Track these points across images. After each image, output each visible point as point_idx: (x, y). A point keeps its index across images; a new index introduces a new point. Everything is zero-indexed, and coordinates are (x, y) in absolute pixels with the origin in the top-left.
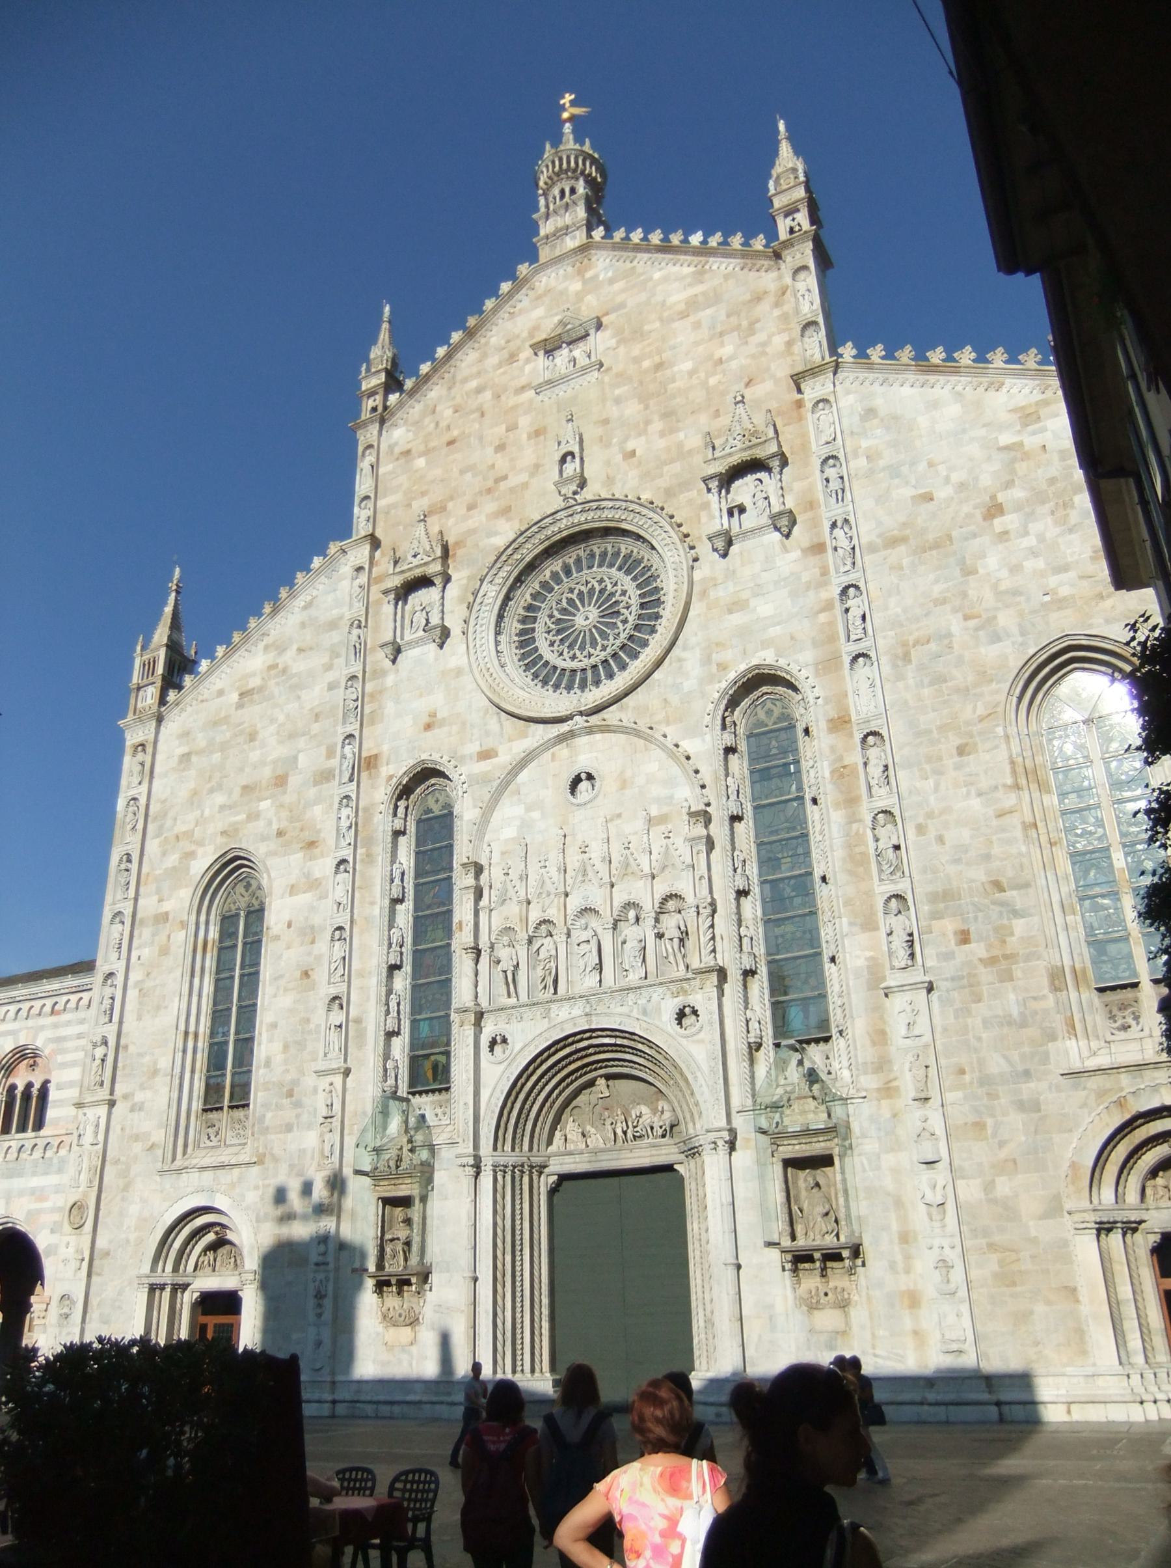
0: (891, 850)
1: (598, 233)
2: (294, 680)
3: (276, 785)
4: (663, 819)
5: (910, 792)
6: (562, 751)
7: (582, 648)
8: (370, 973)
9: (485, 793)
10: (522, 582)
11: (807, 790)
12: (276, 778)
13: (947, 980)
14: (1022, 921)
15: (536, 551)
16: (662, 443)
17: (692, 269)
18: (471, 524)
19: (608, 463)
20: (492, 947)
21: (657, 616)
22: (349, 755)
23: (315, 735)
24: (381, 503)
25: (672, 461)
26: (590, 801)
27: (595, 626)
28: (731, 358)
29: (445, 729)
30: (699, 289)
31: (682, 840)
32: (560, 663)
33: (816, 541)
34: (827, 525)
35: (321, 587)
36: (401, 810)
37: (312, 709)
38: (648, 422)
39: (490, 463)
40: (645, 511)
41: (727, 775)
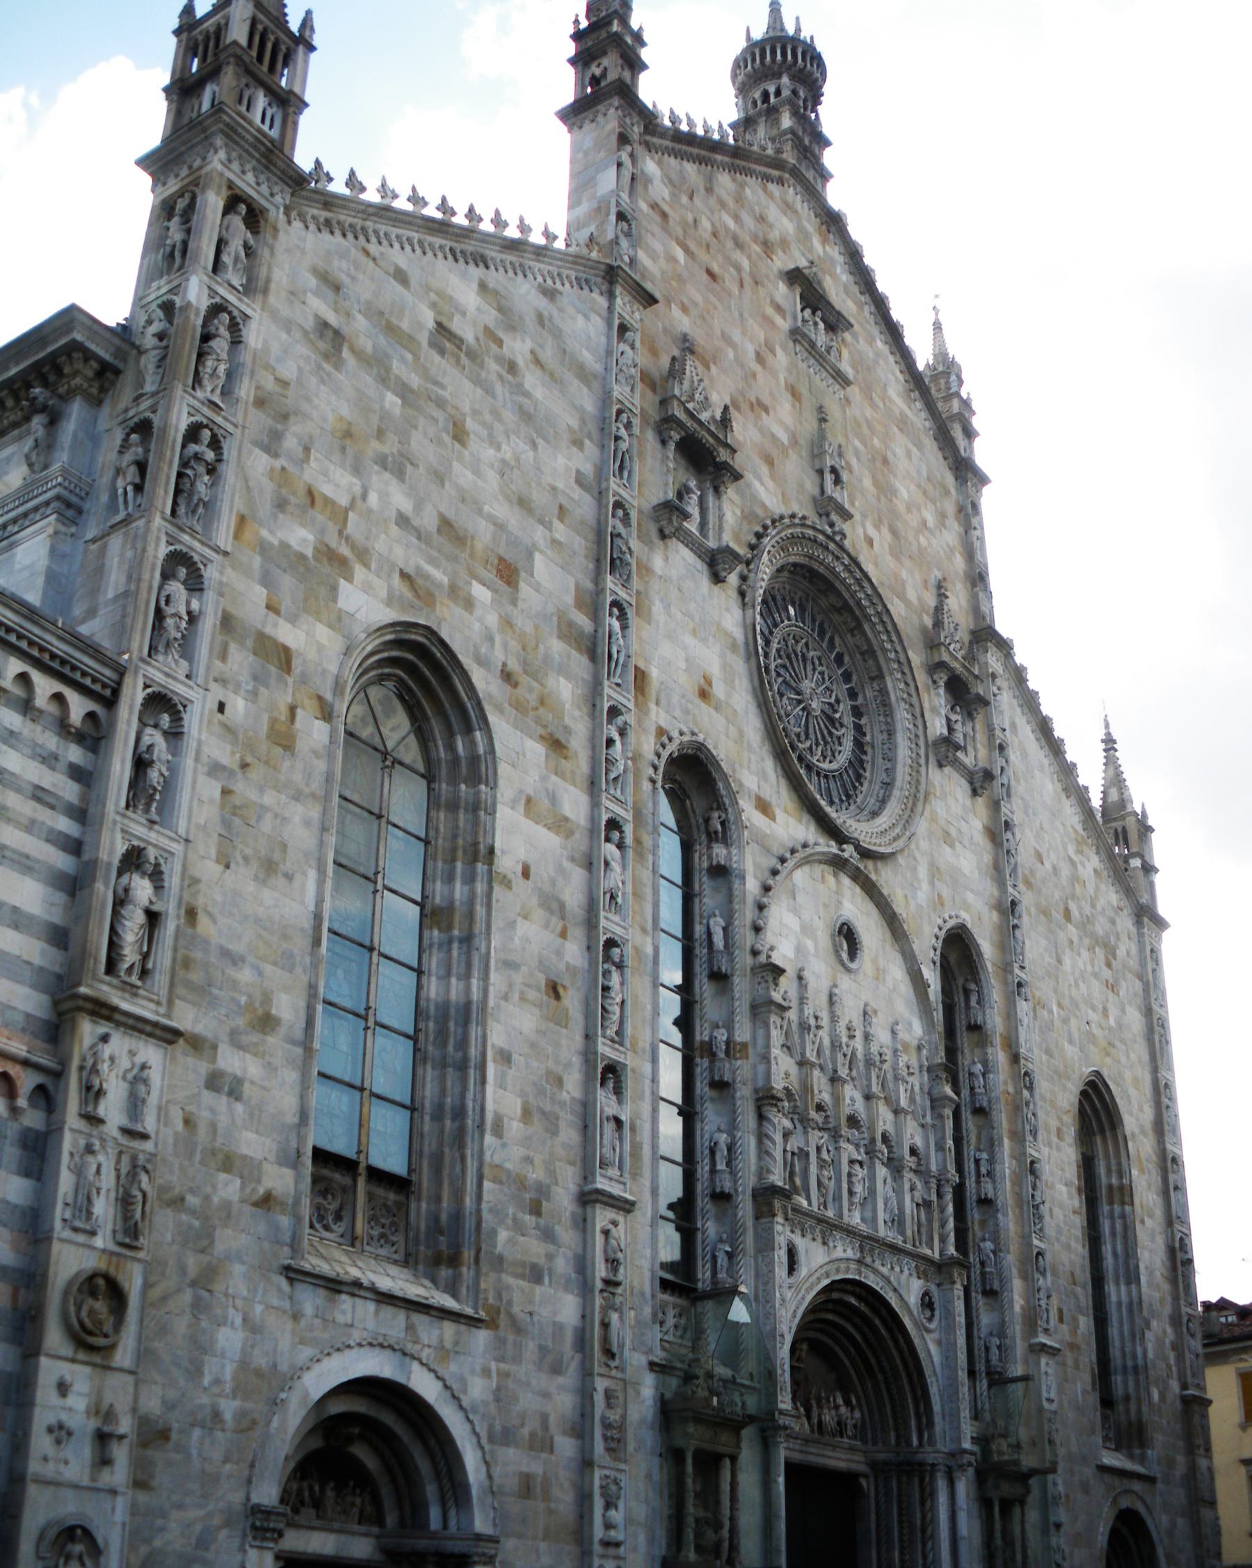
4: (906, 1046)
12: (501, 559)
16: (890, 561)
23: (560, 543)
35: (567, 285)
37: (554, 489)
40: (894, 638)
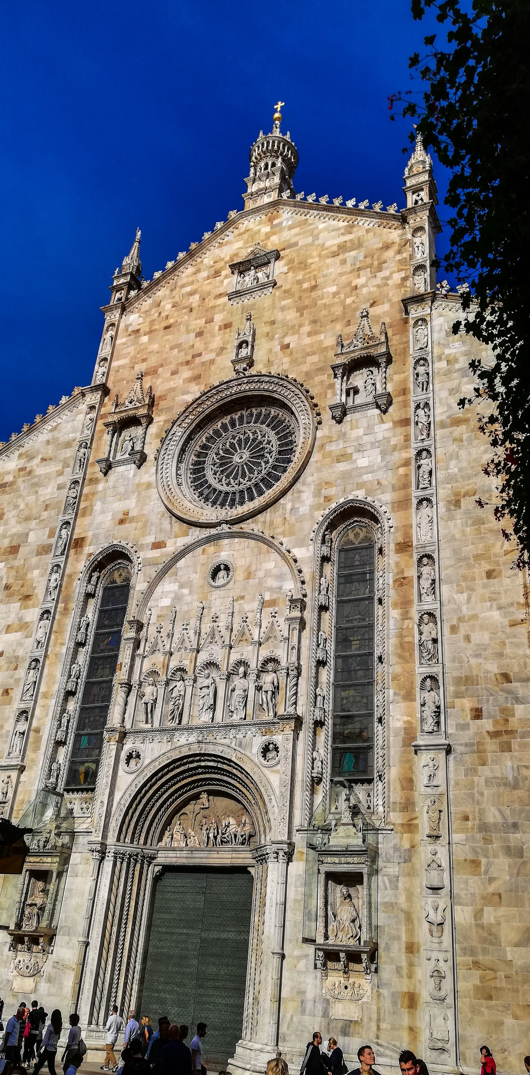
0: (430, 642)
1: (286, 194)
2: (34, 480)
3: (11, 553)
4: (273, 603)
5: (449, 601)
6: (210, 548)
7: (235, 478)
8: (52, 695)
9: (152, 572)
10: (201, 428)
11: (377, 593)
13: (462, 745)
14: (522, 706)
15: (213, 407)
16: (307, 341)
17: (345, 223)
18: (172, 384)
19: (270, 351)
20: (140, 685)
21: (289, 461)
22: (64, 536)
23: (43, 520)
24: (115, 364)
25: (314, 353)
26: (224, 585)
27: (246, 464)
28: (363, 286)
29: (134, 525)
30: (348, 237)
31: (283, 619)
32: (219, 487)
33: (403, 416)
34: (413, 406)
35: (65, 417)
36: (94, 579)
38: (301, 326)
39: (191, 344)
40: (290, 386)
41: (321, 576)
